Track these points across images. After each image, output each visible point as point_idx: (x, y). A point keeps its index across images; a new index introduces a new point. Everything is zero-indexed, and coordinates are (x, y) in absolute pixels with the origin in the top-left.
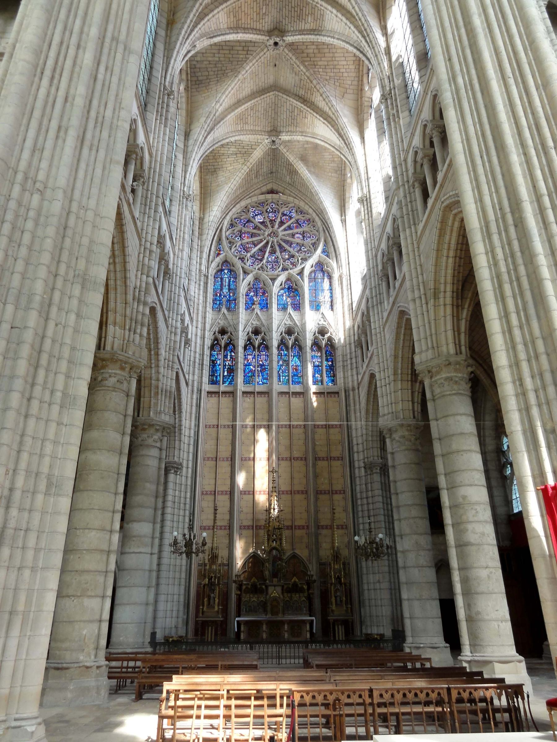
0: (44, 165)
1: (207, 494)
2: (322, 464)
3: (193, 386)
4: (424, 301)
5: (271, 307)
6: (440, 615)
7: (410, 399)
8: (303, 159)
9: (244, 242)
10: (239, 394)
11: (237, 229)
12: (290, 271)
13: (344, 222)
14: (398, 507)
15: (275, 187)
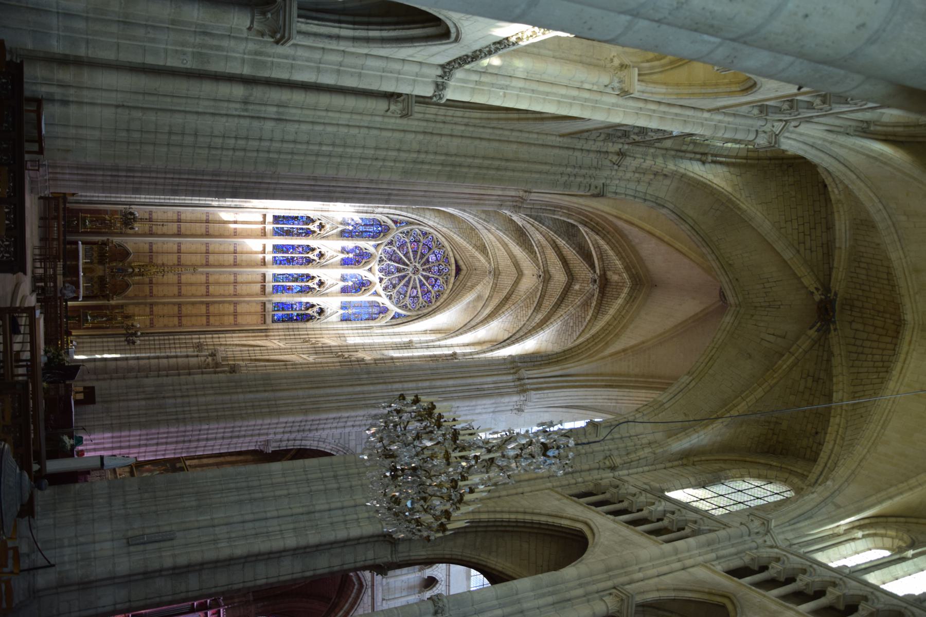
9: (409, 245)
12: (378, 284)
15: (463, 273)
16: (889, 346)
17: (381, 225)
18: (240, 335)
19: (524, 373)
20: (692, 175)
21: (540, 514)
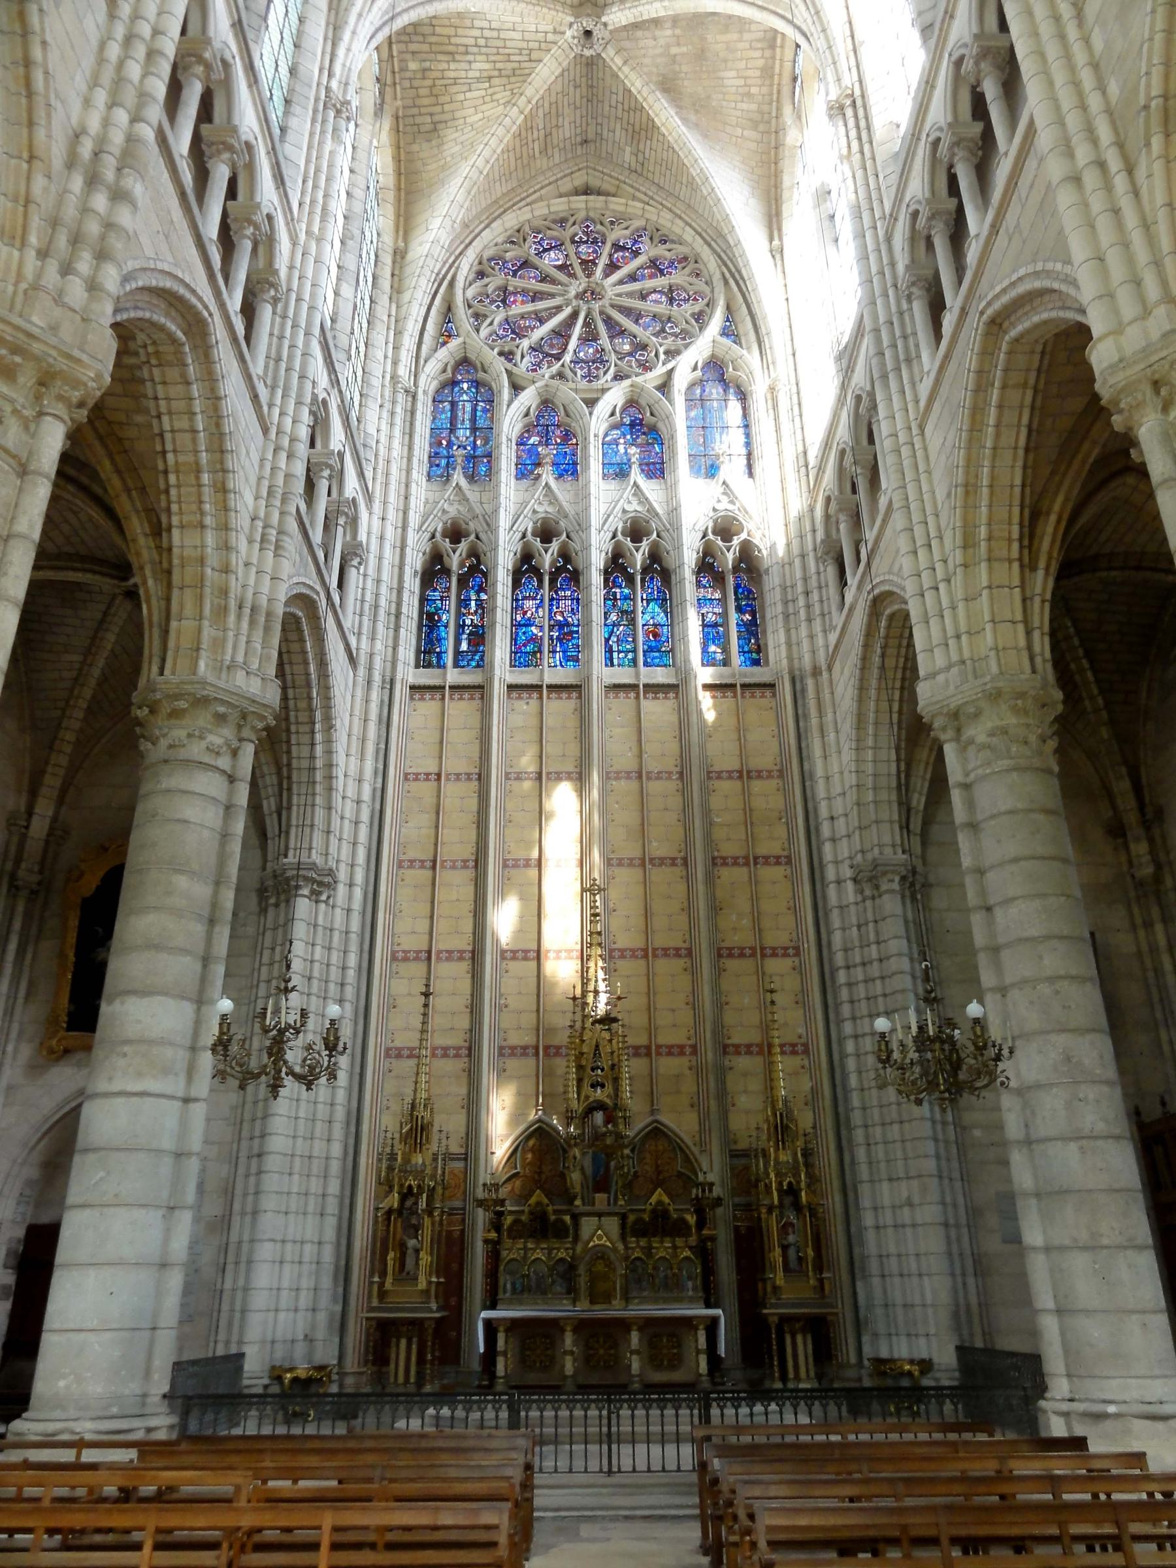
1: (406, 959)
3: (370, 669)
4: (1114, 163)
5: (587, 467)
6: (1162, 1303)
7: (1019, 616)
8: (668, 86)
11: (494, 282)
12: (639, 379)
13: (778, 253)
14: (995, 950)
15: (595, 183)
17: (454, 383)
18: (817, 752)
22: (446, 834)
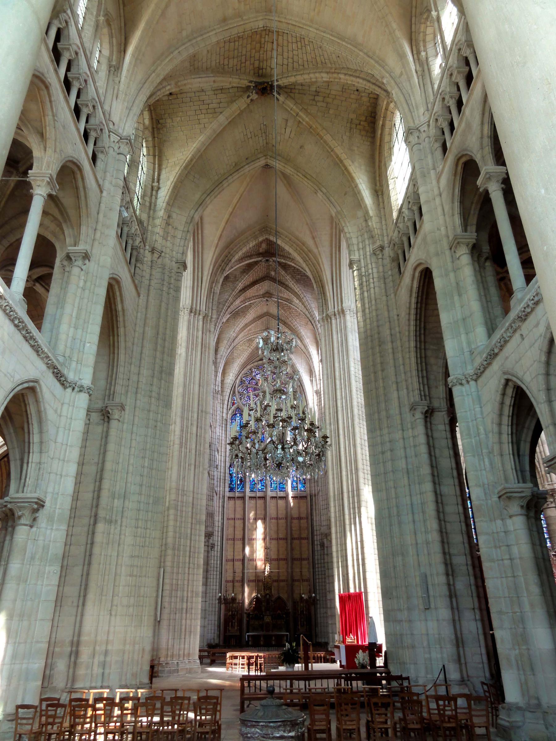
0: (186, 484)
2: (296, 542)
10: (247, 498)
16: (285, 38)
19: (331, 310)
20: (167, 197)
21: (410, 303)
22: (236, 532)
